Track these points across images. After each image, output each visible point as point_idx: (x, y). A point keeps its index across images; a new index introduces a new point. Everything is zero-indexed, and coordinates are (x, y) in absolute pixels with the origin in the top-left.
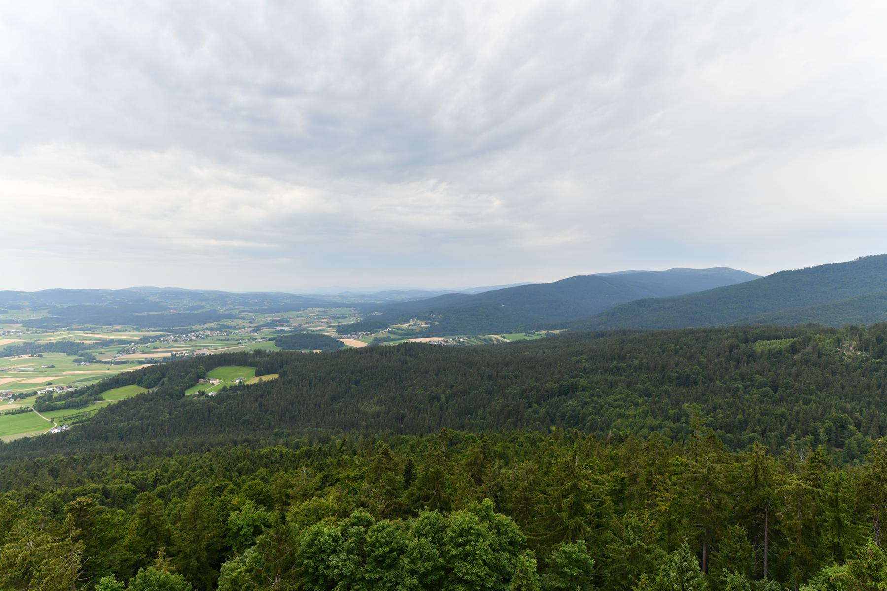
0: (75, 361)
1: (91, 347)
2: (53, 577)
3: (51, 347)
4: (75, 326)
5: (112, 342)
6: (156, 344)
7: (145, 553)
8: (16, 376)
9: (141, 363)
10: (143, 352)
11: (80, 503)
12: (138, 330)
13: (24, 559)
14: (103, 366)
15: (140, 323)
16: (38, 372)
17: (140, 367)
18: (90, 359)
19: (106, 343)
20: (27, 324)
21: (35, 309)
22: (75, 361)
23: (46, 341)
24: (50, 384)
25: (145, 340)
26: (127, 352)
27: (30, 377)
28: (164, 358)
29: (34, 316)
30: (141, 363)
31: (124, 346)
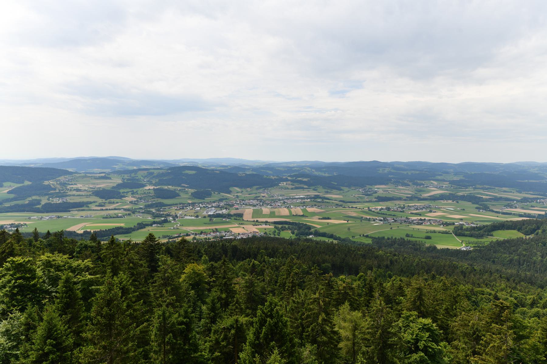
0: (477, 208)
1: (487, 200)
2: (495, 346)
3: (463, 198)
4: (478, 186)
5: (501, 198)
6: (534, 204)
7: (544, 357)
8: (444, 212)
9: (521, 216)
10: (523, 208)
11: (502, 303)
12: (520, 192)
13: (473, 324)
14: (494, 213)
15: (521, 188)
16: (456, 212)
17: (521, 219)
18: (486, 208)
19: (496, 199)
20: (452, 182)
21: (456, 174)
22: (477, 208)
23: (461, 194)
24: (461, 220)
25: (525, 200)
26: (511, 207)
27: (451, 214)
28: (539, 215)
29: (456, 178)
30: (521, 216)
31: (509, 203)
